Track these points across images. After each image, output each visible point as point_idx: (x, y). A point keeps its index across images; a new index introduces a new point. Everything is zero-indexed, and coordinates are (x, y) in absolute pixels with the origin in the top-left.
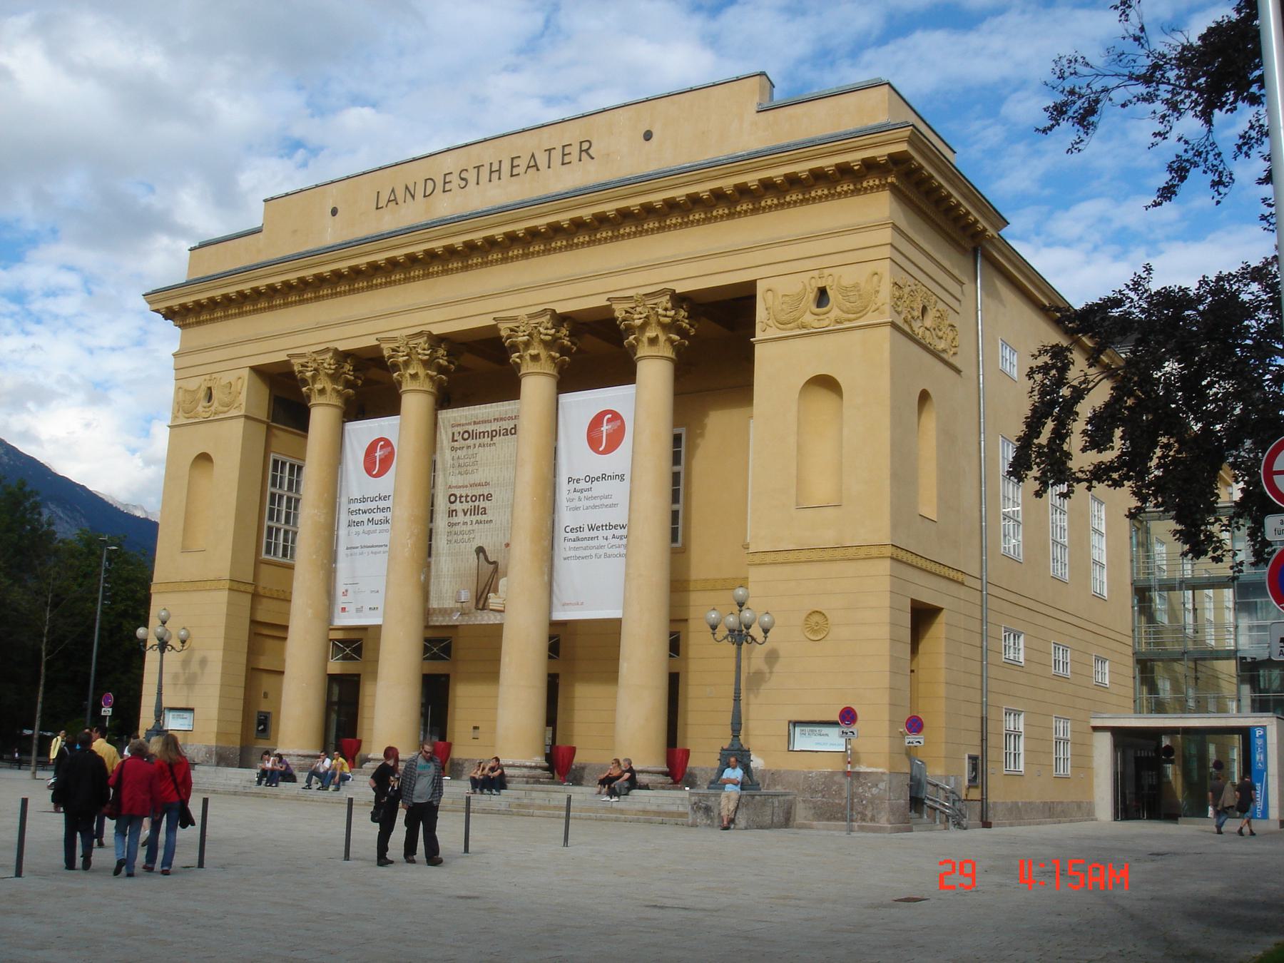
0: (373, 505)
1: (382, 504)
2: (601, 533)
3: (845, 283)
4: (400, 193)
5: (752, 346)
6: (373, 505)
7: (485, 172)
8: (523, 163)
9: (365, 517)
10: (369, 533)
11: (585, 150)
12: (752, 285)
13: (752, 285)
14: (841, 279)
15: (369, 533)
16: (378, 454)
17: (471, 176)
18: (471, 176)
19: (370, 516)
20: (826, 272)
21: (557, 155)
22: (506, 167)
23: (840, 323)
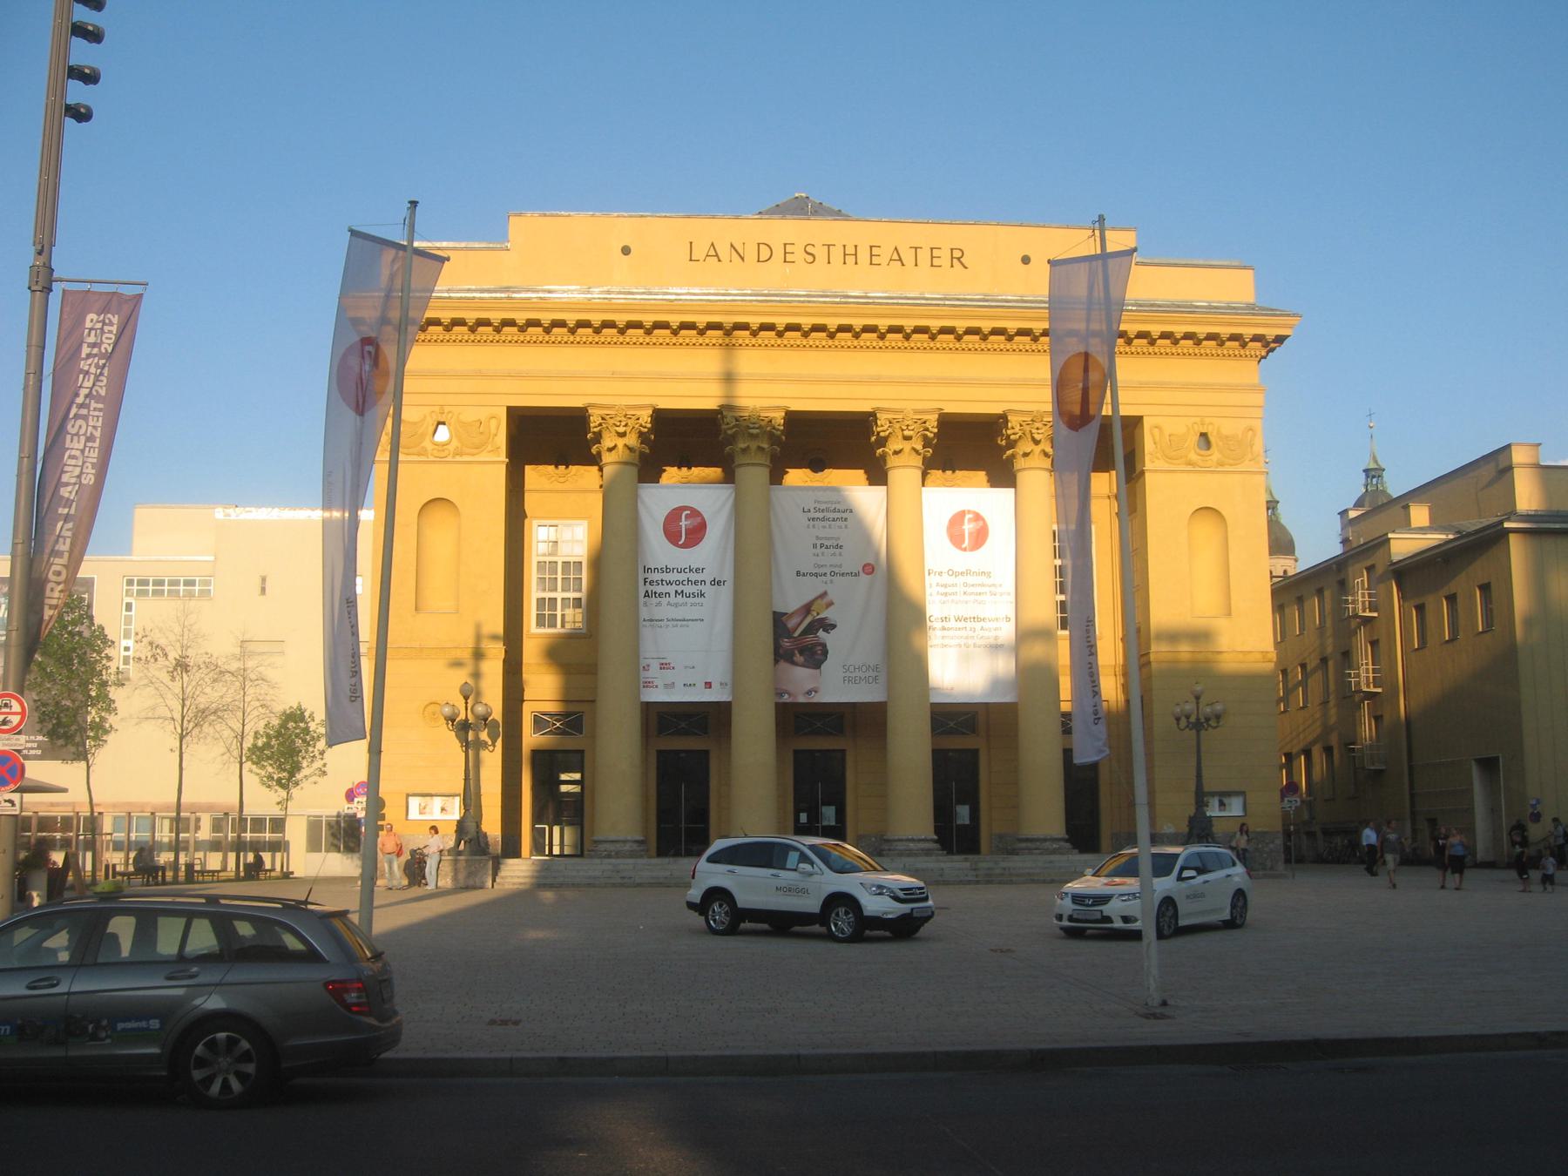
0: (682, 577)
1: (693, 576)
2: (969, 625)
4: (724, 251)
5: (1142, 473)
6: (682, 577)
7: (837, 254)
8: (885, 253)
9: (671, 589)
10: (676, 605)
11: (957, 258)
12: (1140, 418)
13: (1140, 418)
14: (1221, 427)
15: (676, 605)
16: (683, 523)
17: (820, 253)
18: (820, 253)
19: (679, 589)
20: (1207, 420)
21: (924, 256)
22: (864, 255)
23: (1222, 465)
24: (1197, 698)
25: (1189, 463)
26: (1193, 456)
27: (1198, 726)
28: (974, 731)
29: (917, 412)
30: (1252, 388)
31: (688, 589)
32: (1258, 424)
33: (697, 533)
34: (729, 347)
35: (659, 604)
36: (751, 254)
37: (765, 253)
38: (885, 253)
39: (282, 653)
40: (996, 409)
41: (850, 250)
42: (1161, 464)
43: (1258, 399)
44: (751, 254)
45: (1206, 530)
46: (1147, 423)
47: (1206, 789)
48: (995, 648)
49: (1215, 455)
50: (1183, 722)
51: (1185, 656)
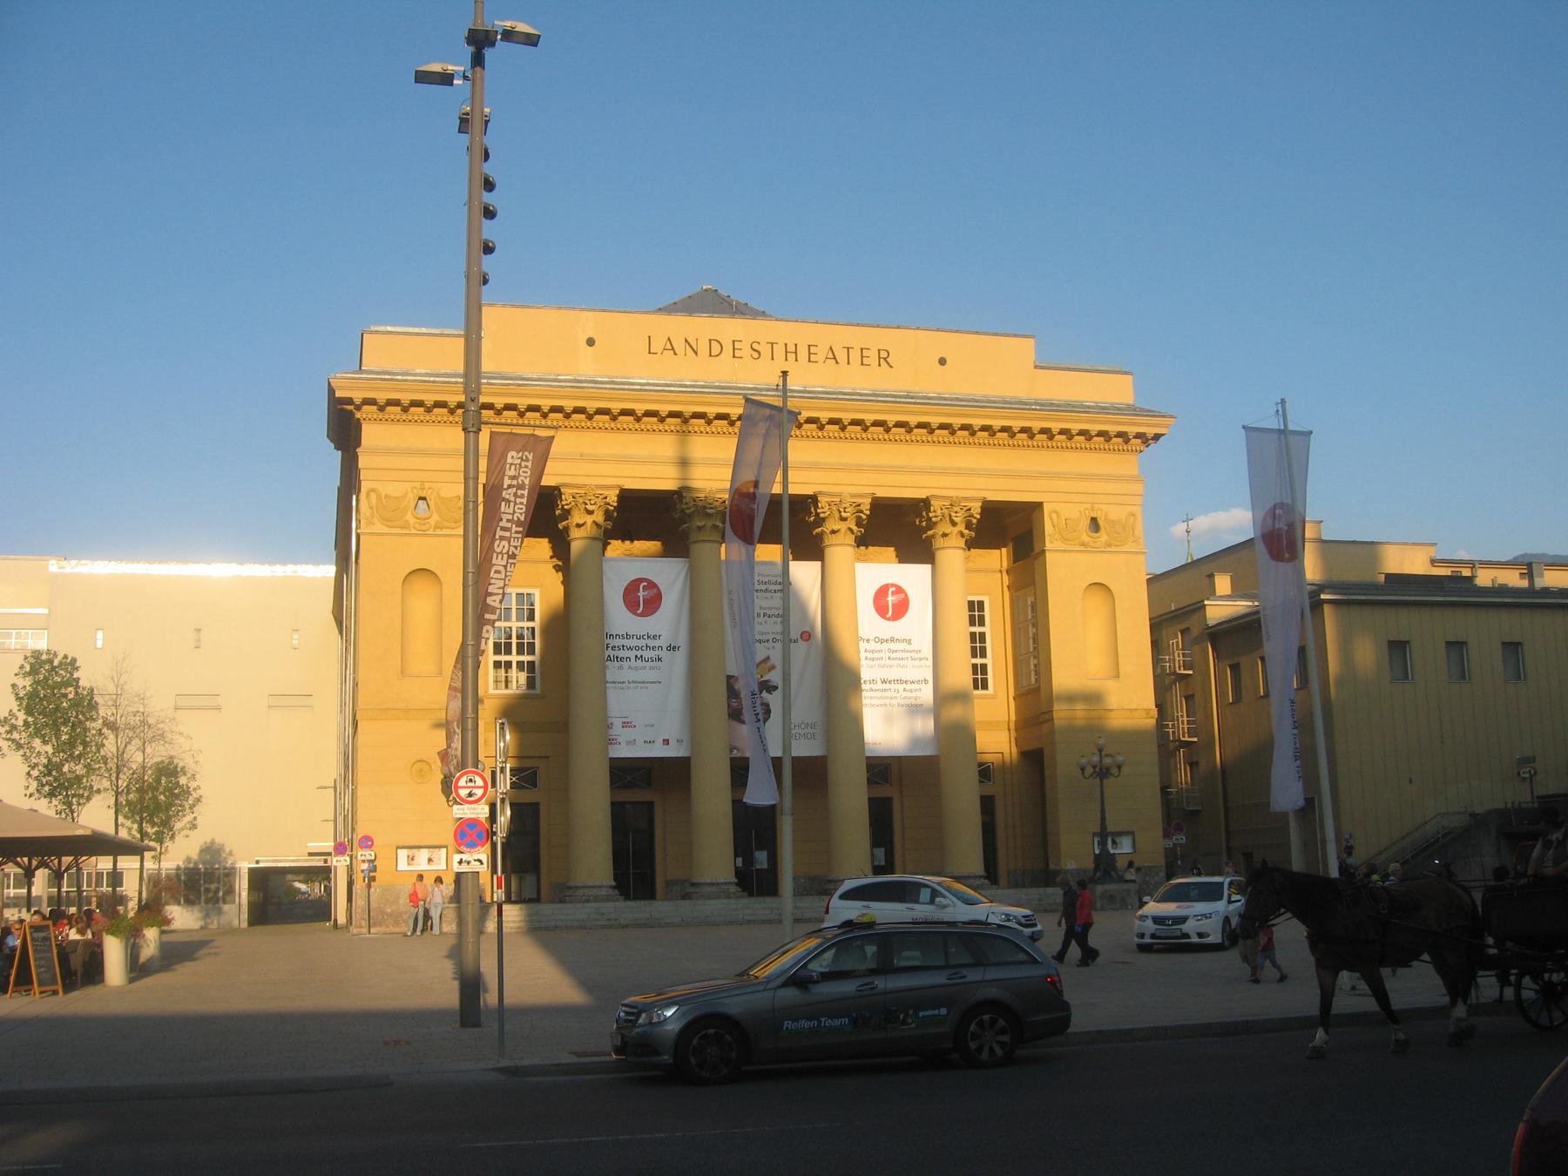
0: (641, 643)
1: (651, 643)
2: (893, 686)
3: (1110, 517)
4: (679, 345)
6: (641, 643)
8: (822, 352)
9: (632, 654)
11: (884, 358)
12: (1039, 505)
14: (1110, 512)
16: (641, 594)
17: (765, 350)
18: (765, 350)
19: (639, 653)
22: (803, 353)
24: (1100, 750)
25: (1083, 544)
26: (1085, 538)
27: (1102, 773)
28: (886, 781)
29: (853, 496)
30: (1134, 479)
31: (647, 654)
32: (1138, 510)
33: (653, 603)
34: (683, 433)
35: (621, 668)
36: (703, 348)
37: (716, 349)
38: (822, 352)
39: (218, 708)
40: (922, 494)
41: (791, 348)
42: (1058, 545)
43: (1137, 488)
44: (703, 348)
45: (1096, 601)
46: (1047, 508)
47: (1110, 828)
48: (914, 709)
49: (1103, 537)
50: (1089, 770)
51: (1080, 714)
